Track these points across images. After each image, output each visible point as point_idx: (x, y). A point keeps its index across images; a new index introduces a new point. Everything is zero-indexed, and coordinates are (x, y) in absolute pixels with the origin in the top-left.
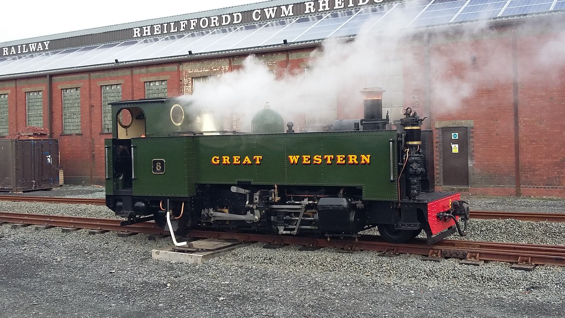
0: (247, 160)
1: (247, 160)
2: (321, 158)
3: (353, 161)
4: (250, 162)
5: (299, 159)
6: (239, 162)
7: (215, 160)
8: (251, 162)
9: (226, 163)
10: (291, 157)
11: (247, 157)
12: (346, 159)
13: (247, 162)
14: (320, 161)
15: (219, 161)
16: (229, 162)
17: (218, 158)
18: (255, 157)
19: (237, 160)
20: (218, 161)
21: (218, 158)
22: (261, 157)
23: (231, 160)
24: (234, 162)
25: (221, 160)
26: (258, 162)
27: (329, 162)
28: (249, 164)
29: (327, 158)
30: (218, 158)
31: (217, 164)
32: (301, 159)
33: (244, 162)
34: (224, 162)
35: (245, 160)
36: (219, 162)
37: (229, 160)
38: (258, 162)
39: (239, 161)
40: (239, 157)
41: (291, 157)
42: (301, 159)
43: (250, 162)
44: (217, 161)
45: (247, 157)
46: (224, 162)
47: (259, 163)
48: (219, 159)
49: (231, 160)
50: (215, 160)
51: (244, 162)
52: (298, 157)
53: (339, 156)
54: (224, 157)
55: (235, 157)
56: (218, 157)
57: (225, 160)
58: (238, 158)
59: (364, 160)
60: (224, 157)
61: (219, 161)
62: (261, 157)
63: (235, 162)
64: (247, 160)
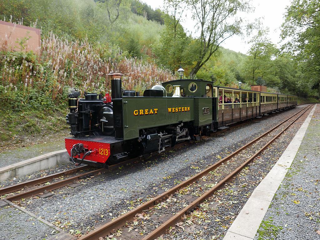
1: (151, 112)
4: (152, 113)
6: (148, 113)
10: (169, 109)
12: (184, 109)
13: (151, 113)
14: (177, 110)
18: (155, 109)
20: (137, 113)
21: (137, 111)
22: (157, 109)
23: (144, 112)
25: (139, 112)
27: (180, 111)
32: (172, 110)
33: (150, 113)
34: (141, 114)
35: (150, 112)
38: (156, 112)
40: (148, 110)
41: (169, 109)
42: (172, 110)
49: (144, 112)
50: (136, 112)
51: (150, 113)
52: (171, 108)
53: (182, 108)
54: (140, 110)
55: (146, 110)
57: (141, 112)
60: (140, 110)
62: (157, 109)
63: (146, 113)
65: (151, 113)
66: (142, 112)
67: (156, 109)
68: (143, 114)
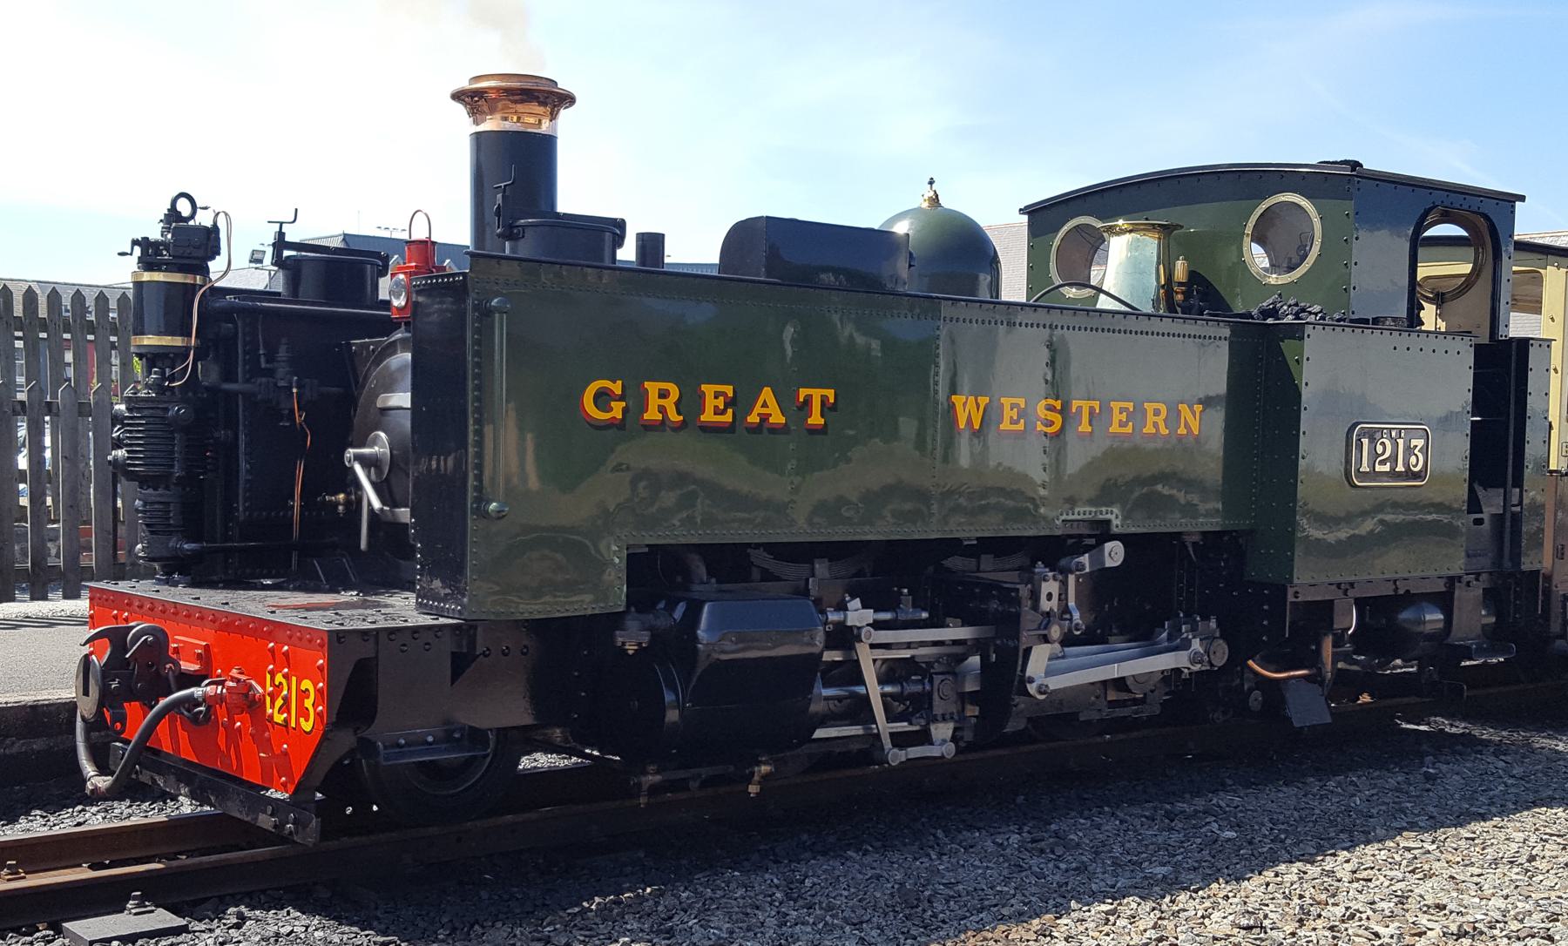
0: (765, 405)
2: (1061, 412)
3: (662, 410)
4: (777, 418)
5: (681, 407)
7: (602, 398)
8: (783, 420)
9: (660, 417)
11: (767, 394)
13: (764, 418)
15: (624, 404)
16: (679, 413)
17: (617, 388)
18: (803, 392)
19: (716, 402)
20: (617, 409)
21: (617, 388)
22: (830, 394)
23: (690, 403)
24: (703, 418)
26: (816, 419)
28: (774, 430)
29: (1080, 408)
30: (618, 391)
31: (611, 424)
33: (753, 418)
34: (652, 415)
35: (758, 409)
36: (625, 411)
37: (677, 404)
38: (816, 419)
39: (730, 411)
40: (729, 390)
43: (777, 418)
44: (613, 404)
45: (767, 394)
46: (652, 415)
47: (822, 421)
48: (621, 398)
50: (602, 398)
51: (753, 418)
54: (652, 388)
55: (708, 389)
56: (619, 382)
57: (654, 401)
58: (724, 394)
59: (1187, 425)
60: (652, 388)
61: (624, 404)
62: (830, 394)
63: (708, 416)
64: (768, 406)
65: (764, 418)
66: (669, 404)
67: (817, 394)
68: (674, 417)
